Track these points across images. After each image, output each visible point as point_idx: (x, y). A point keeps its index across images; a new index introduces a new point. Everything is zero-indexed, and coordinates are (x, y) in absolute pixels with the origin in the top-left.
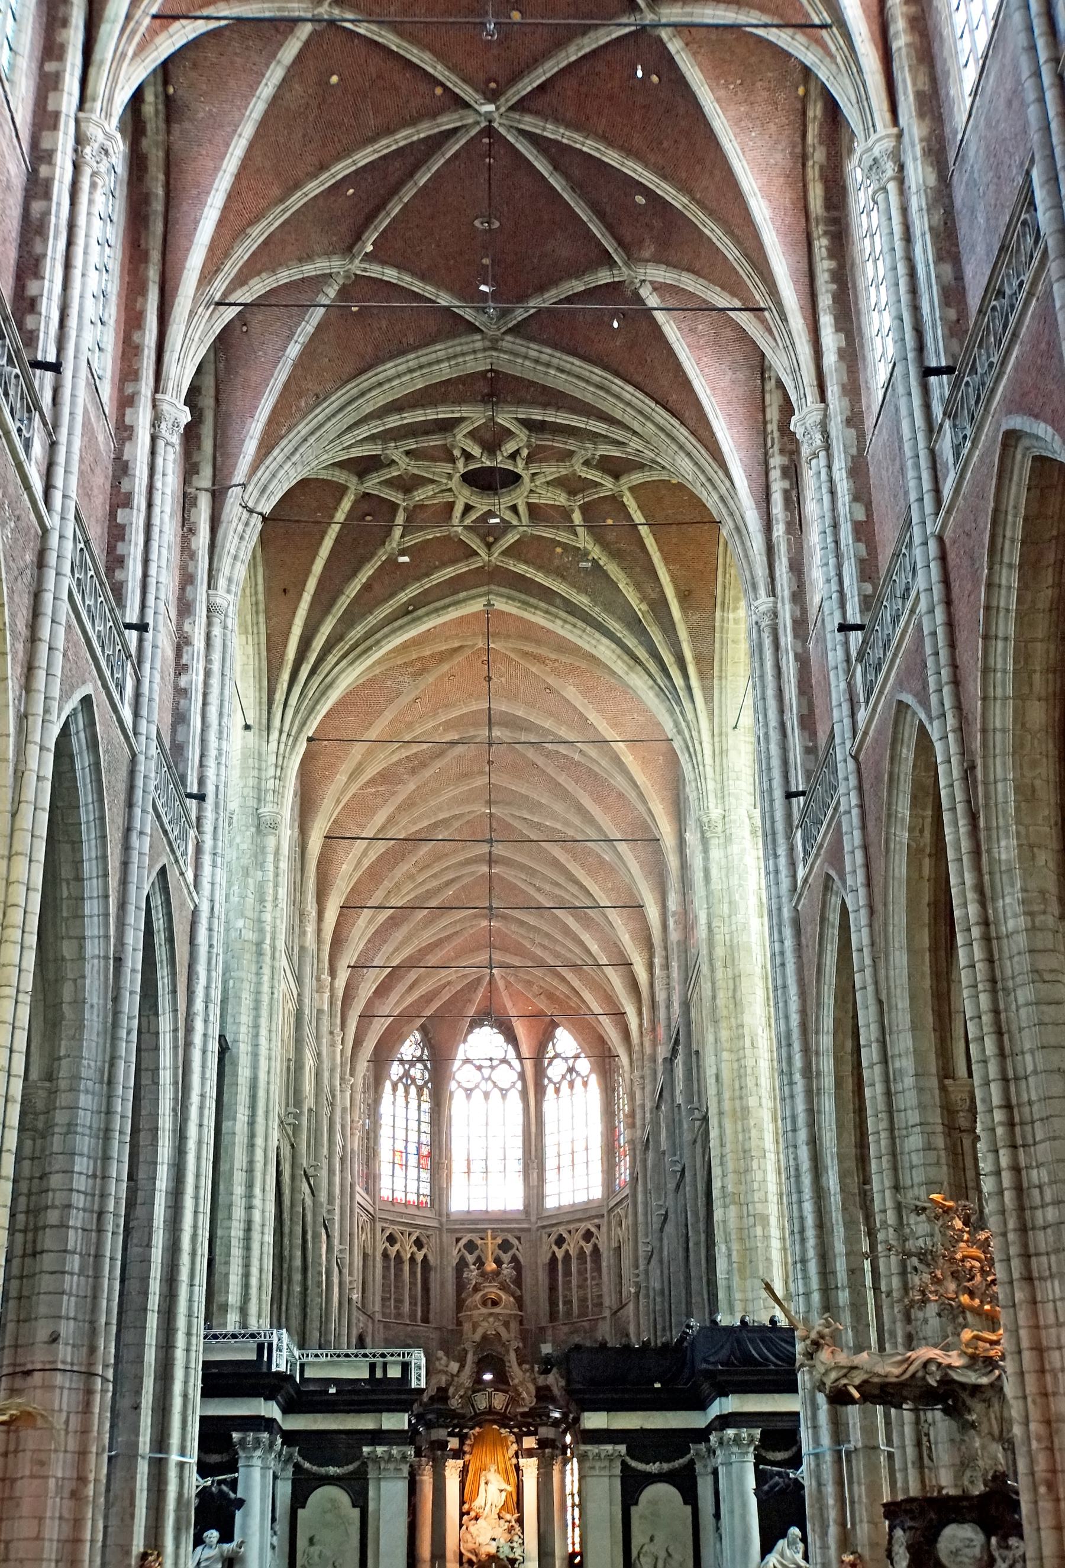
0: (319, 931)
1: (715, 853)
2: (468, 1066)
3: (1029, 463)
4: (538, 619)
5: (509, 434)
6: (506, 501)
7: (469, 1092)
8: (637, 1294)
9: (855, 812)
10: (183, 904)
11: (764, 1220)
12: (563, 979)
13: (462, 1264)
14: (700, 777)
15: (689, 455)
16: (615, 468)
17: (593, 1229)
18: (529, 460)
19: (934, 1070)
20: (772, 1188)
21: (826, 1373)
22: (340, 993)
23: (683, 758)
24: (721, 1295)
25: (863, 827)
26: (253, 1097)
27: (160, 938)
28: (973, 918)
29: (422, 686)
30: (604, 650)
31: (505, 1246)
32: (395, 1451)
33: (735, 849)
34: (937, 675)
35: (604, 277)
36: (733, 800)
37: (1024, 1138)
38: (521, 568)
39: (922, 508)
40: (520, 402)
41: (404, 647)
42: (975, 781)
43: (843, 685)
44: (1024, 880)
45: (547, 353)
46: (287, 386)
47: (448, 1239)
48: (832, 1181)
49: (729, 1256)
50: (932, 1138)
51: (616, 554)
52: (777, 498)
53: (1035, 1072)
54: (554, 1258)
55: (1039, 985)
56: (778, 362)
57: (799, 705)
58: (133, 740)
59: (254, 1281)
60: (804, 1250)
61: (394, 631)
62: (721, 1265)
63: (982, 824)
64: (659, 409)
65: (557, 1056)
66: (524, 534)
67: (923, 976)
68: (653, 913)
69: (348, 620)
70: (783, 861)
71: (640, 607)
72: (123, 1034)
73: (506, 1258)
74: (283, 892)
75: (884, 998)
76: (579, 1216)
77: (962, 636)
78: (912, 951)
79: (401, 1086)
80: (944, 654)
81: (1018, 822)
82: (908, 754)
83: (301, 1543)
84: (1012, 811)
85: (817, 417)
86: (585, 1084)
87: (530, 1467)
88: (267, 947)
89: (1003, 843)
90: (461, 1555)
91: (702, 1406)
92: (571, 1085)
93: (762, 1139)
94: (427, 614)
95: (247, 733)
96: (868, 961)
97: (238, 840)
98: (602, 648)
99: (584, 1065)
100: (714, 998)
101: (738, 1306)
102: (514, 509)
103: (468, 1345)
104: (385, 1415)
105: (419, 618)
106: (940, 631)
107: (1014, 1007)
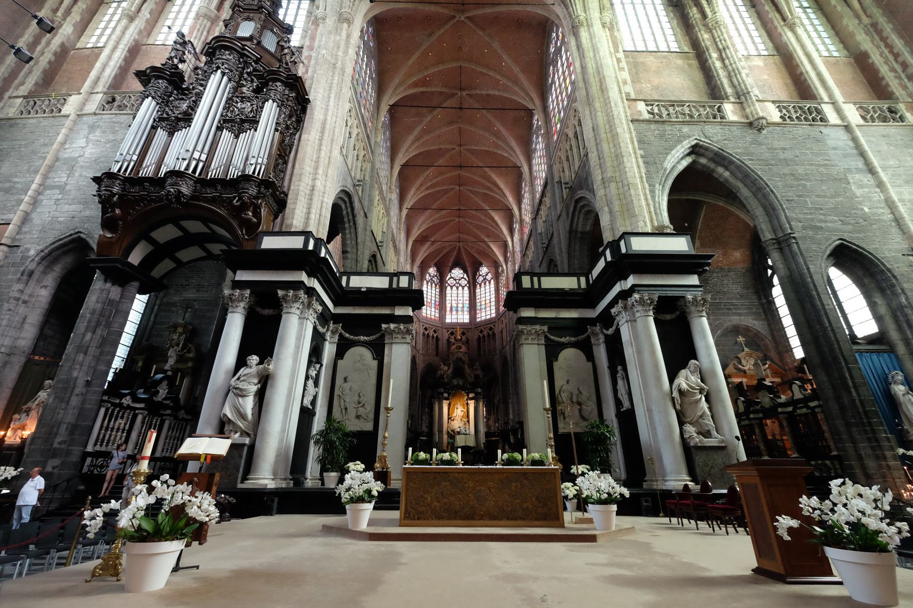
7: (452, 287)
13: (449, 338)
26: (323, 128)
47: (445, 331)
54: (479, 337)
59: (312, 216)
65: (480, 275)
79: (429, 284)
83: (339, 381)
87: (472, 404)
88: (339, 65)
90: (448, 432)
92: (485, 284)
99: (489, 277)
103: (451, 362)
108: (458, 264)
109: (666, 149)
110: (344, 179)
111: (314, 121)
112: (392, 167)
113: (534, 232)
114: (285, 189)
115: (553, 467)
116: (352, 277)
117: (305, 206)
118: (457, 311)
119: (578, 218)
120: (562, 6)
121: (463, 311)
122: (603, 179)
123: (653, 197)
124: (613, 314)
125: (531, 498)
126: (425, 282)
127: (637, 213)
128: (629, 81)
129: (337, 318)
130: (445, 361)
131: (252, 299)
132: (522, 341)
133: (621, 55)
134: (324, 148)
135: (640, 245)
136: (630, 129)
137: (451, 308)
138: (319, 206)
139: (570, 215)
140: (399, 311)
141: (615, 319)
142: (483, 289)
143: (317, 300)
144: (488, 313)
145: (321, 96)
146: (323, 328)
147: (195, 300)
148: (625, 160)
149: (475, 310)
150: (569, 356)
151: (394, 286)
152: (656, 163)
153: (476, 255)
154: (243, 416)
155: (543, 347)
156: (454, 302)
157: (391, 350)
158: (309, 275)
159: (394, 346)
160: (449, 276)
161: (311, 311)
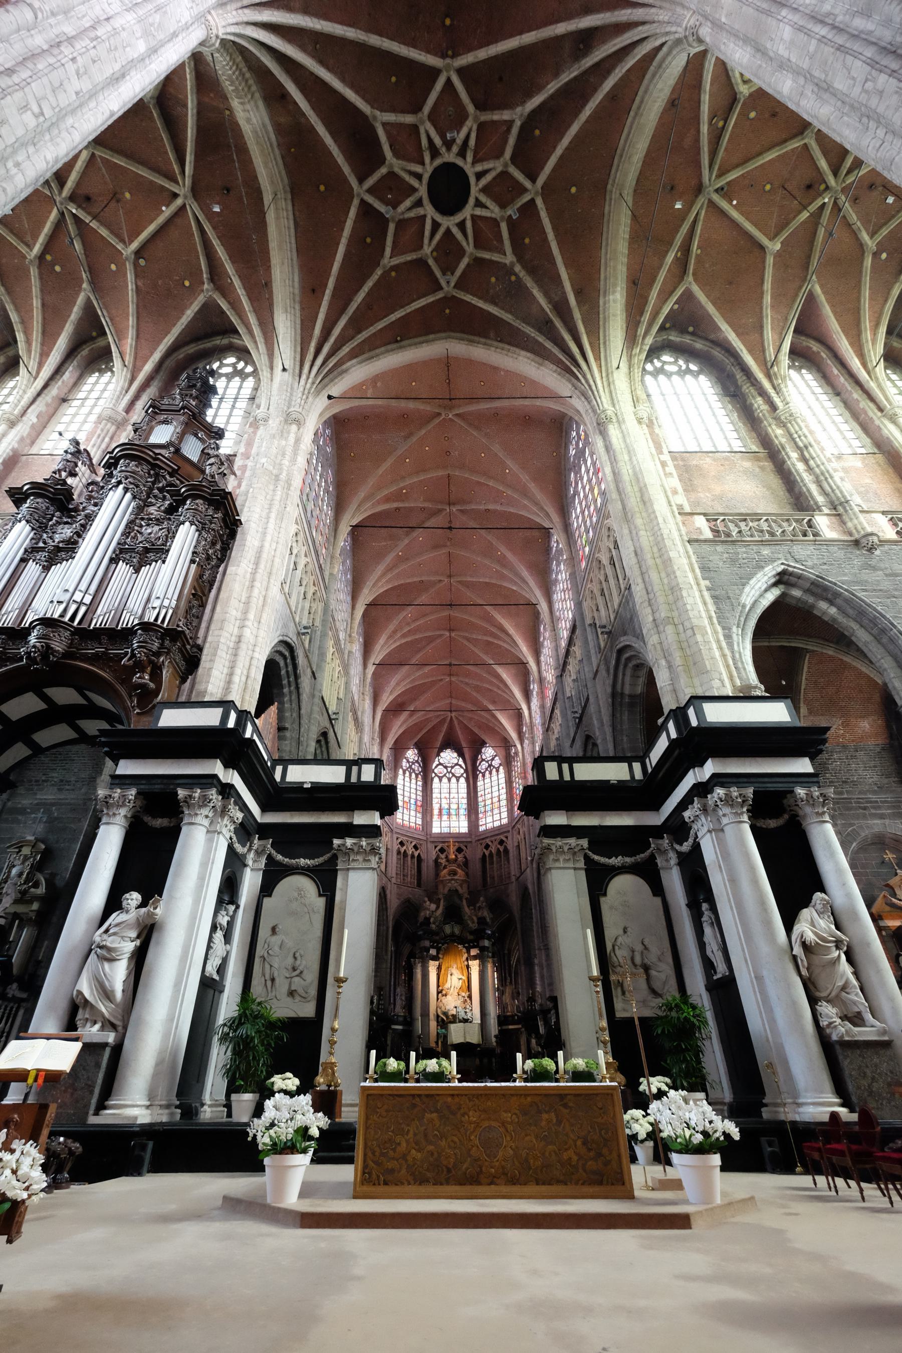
2: (440, 767)
7: (440, 779)
13: (438, 857)
17: (504, 839)
32: (364, 843)
51: (532, 271)
59: (236, 679)
65: (483, 760)
79: (407, 774)
86: (497, 771)
87: (475, 965)
88: (283, 476)
90: (438, 1016)
92: (491, 773)
94: (410, 345)
95: (284, 373)
98: (521, 358)
99: (496, 762)
103: (441, 896)
104: (356, 812)
108: (450, 743)
109: (741, 578)
110: (285, 626)
111: (246, 549)
112: (353, 607)
113: (560, 696)
114: (199, 642)
115: (608, 1083)
116: (290, 767)
117: (227, 664)
118: (449, 814)
119: (624, 675)
120: (583, 399)
121: (458, 815)
122: (654, 620)
123: (730, 645)
124: (687, 820)
125: (575, 1141)
126: (401, 771)
127: (709, 668)
128: (680, 489)
129: (264, 831)
130: (432, 896)
131: (139, 803)
132: (550, 863)
133: (666, 457)
134: (257, 584)
136: (687, 552)
137: (440, 810)
138: (247, 664)
139: (612, 671)
140: (361, 818)
141: (691, 828)
142: (487, 780)
143: (236, 803)
144: (497, 817)
145: (257, 516)
146: (244, 846)
147: (53, 804)
148: (684, 593)
149: (477, 813)
151: (354, 779)
152: (729, 598)
153: (476, 730)
154: (107, 994)
155: (583, 873)
156: (444, 801)
157: (346, 879)
158: (226, 766)
159: (351, 874)
160: (436, 762)
161: (226, 821)
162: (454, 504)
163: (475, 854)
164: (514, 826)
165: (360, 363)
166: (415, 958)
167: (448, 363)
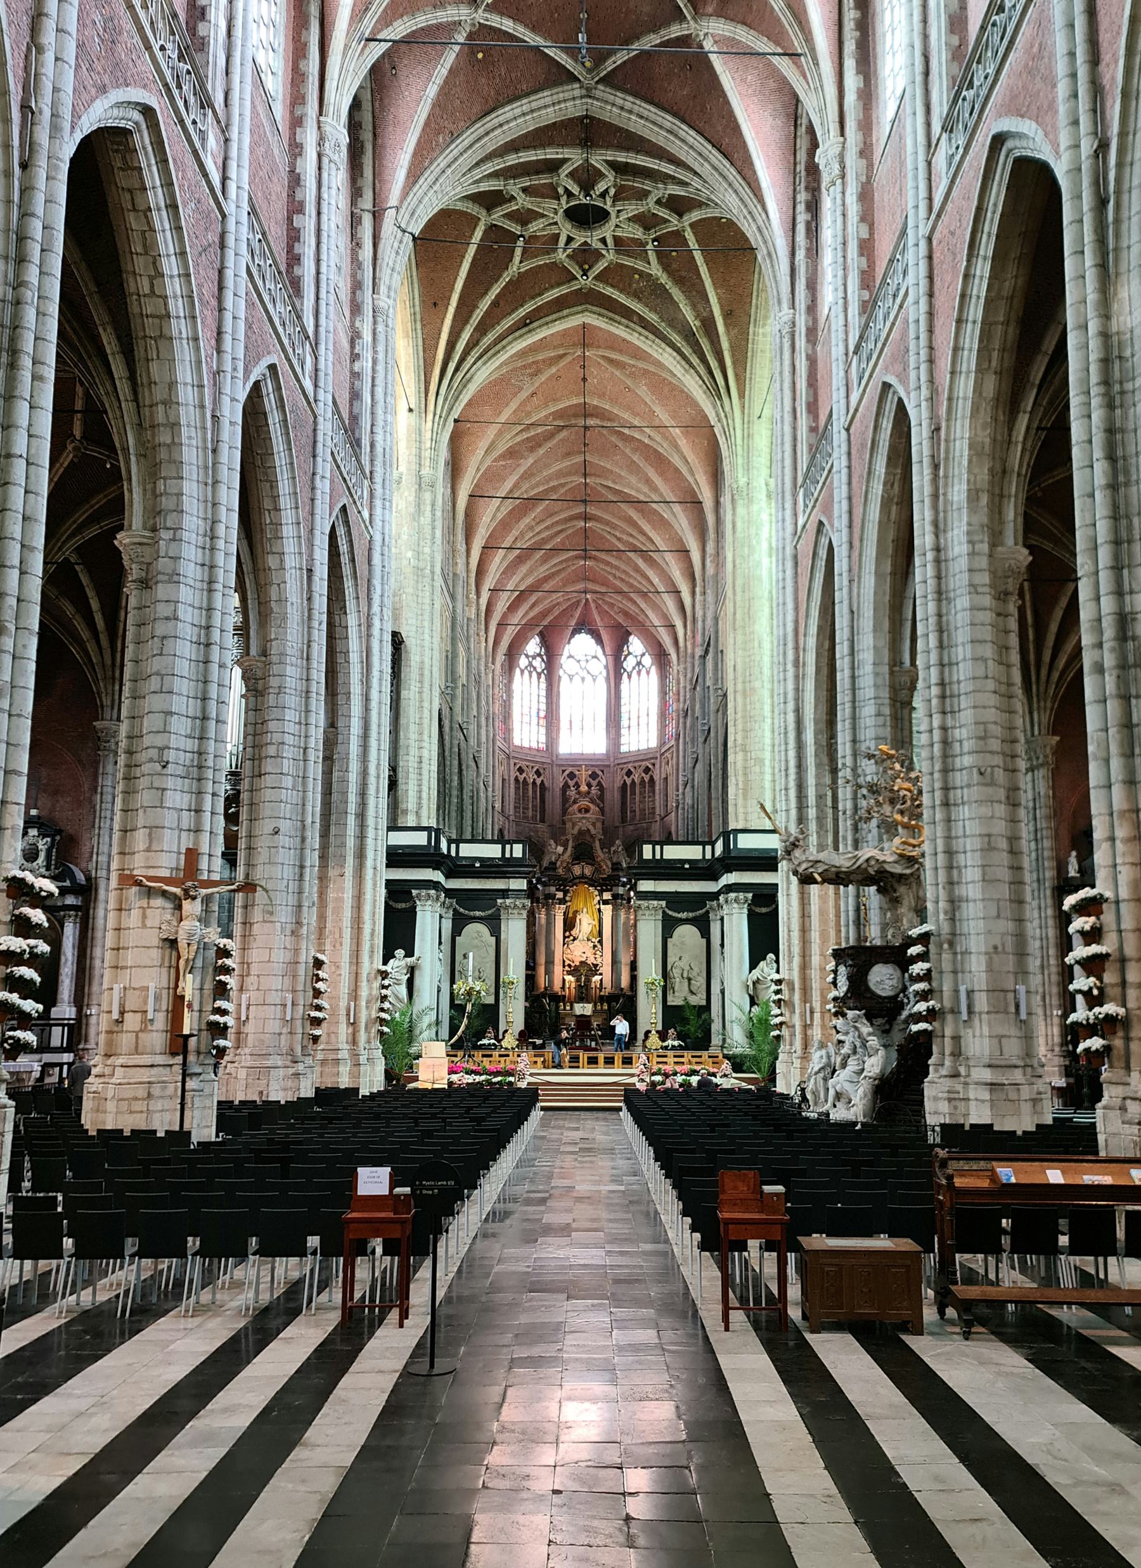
0: (468, 563)
1: (741, 511)
3: (1010, 161)
4: (620, 331)
5: (601, 175)
6: (598, 234)
7: (571, 677)
8: (677, 807)
9: (845, 471)
10: (361, 535)
11: (760, 761)
12: (635, 603)
13: (566, 786)
14: (734, 454)
15: (735, 191)
16: (679, 206)
18: (616, 199)
19: (886, 660)
20: (768, 741)
21: (799, 864)
22: (483, 608)
23: (721, 440)
24: (731, 809)
25: (850, 483)
27: (345, 559)
28: (929, 545)
29: (537, 385)
30: (667, 357)
31: (594, 776)
33: (755, 508)
34: (917, 357)
35: (675, 31)
36: (755, 472)
37: (952, 706)
38: (609, 291)
39: (917, 215)
40: (608, 146)
41: (522, 354)
42: (939, 439)
43: (842, 373)
44: (969, 516)
45: (629, 101)
46: (427, 124)
48: (809, 737)
49: (737, 784)
50: (882, 708)
51: (679, 281)
52: (801, 228)
53: (964, 659)
55: (974, 596)
56: (809, 103)
57: (807, 394)
58: (313, 405)
60: (787, 783)
61: (516, 339)
62: (731, 790)
63: (941, 473)
64: (714, 151)
66: (611, 263)
67: (884, 594)
68: (696, 556)
69: (482, 329)
70: (788, 513)
71: (694, 323)
72: (315, 624)
73: (594, 783)
74: (438, 533)
75: (855, 609)
76: (641, 758)
77: (938, 323)
78: (878, 575)
80: (923, 336)
81: (969, 471)
82: (887, 425)
84: (965, 463)
85: (837, 150)
86: (648, 673)
89: (956, 488)
91: (715, 878)
92: (639, 673)
93: (762, 709)
94: (540, 327)
96: (845, 583)
97: (406, 494)
98: (666, 355)
99: (647, 660)
100: (735, 614)
101: (741, 817)
102: (603, 241)
103: (570, 837)
105: (534, 330)
106: (923, 319)
107: (953, 611)
130: (558, 834)
135: (746, 842)
150: (687, 934)
160: (566, 653)
162: (592, 415)
163: (613, 782)
164: (663, 754)
165: (485, 364)
166: (538, 902)
167: (584, 326)
